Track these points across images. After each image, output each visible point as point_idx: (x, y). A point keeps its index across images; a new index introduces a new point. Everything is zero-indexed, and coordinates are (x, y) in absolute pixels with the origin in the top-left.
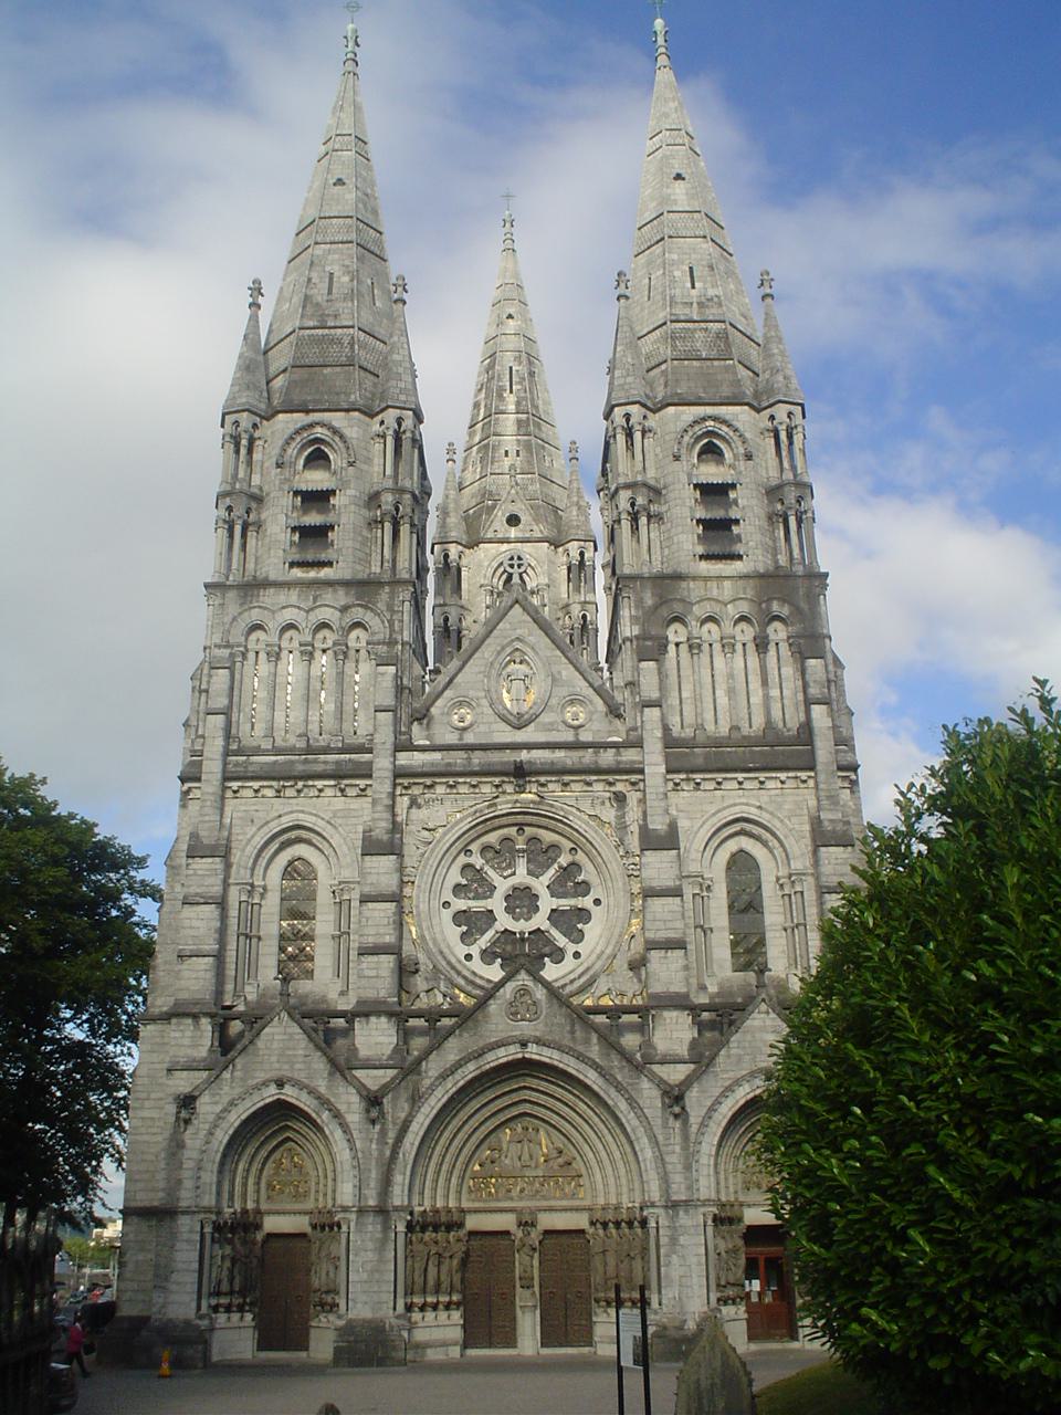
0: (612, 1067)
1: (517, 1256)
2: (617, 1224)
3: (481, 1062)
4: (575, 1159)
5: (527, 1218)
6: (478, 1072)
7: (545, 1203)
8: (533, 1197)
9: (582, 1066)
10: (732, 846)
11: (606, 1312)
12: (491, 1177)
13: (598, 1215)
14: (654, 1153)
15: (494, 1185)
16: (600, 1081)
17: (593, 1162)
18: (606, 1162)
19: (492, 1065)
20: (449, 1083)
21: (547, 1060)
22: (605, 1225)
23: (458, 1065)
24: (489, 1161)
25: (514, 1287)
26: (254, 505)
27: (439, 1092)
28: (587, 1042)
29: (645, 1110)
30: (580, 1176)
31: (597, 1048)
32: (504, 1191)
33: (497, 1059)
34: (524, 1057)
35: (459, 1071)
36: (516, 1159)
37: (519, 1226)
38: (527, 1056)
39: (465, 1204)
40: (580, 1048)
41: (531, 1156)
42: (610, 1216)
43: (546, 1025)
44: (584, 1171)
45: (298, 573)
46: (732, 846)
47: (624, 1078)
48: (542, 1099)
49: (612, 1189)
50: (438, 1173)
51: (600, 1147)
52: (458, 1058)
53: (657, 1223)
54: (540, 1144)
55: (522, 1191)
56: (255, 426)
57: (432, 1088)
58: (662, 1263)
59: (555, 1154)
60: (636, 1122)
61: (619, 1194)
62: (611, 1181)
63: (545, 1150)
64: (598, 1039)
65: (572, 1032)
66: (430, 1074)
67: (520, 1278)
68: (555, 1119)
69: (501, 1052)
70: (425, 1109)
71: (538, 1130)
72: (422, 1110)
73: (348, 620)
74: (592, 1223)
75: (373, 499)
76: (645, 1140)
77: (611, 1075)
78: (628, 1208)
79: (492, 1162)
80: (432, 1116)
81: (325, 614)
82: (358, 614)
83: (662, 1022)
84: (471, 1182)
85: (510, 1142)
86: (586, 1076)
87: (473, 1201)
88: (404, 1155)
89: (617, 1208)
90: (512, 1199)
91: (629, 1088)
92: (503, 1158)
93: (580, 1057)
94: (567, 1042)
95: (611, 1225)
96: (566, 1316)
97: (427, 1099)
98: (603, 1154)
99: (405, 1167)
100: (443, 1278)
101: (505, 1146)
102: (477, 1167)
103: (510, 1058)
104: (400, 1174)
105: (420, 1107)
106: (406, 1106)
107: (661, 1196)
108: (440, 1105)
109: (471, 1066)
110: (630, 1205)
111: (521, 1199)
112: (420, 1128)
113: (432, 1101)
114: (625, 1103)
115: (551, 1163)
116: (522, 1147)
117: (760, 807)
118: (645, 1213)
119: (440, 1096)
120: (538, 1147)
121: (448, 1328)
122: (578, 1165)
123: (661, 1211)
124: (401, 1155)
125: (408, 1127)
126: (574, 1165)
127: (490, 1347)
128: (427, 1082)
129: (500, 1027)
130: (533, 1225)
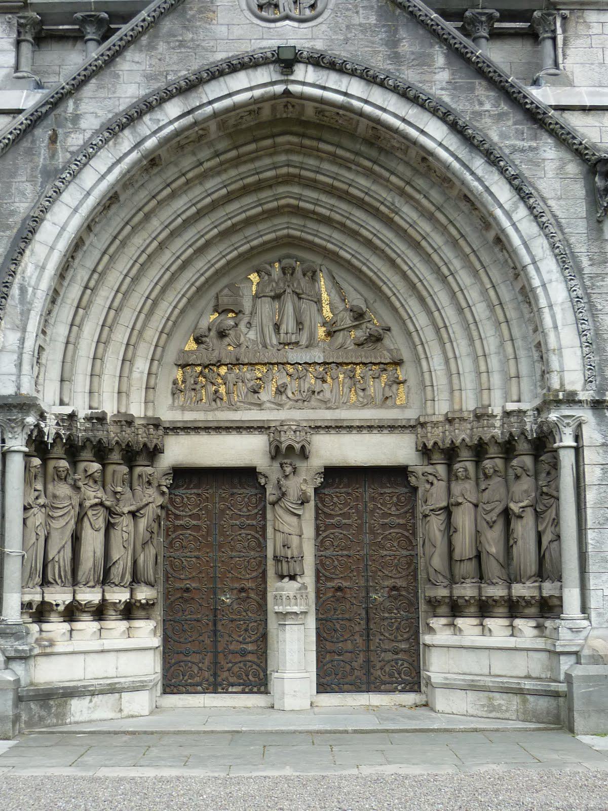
0: (478, 115)
1: (269, 516)
2: (479, 450)
3: (194, 100)
4: (389, 330)
5: (287, 439)
6: (189, 119)
7: (327, 415)
8: (303, 401)
9: (412, 113)
11: (452, 625)
12: (219, 364)
13: (434, 436)
14: (570, 290)
15: (224, 378)
16: (453, 142)
17: (428, 334)
18: (456, 330)
19: (217, 106)
20: (127, 140)
21: (340, 98)
22: (451, 454)
23: (146, 107)
24: (213, 333)
25: (264, 574)
27: (101, 162)
28: (423, 61)
29: (551, 203)
30: (398, 363)
31: (444, 76)
32: (243, 389)
33: (230, 95)
34: (287, 93)
35: (146, 118)
36: (269, 329)
37: (273, 458)
38: (295, 88)
39: (167, 415)
40: (410, 76)
41: (299, 324)
42: (462, 434)
43: (335, 28)
44: (406, 355)
47: (503, 136)
48: (326, 204)
49: (468, 381)
50: (102, 342)
51: (443, 298)
52: (143, 92)
53: (578, 438)
54: (318, 302)
55: (280, 391)
57: (87, 153)
58: (590, 524)
59: (347, 320)
60: (529, 227)
61: (482, 389)
62: (466, 364)
63: (327, 312)
64: (447, 56)
65: (392, 43)
66: (83, 124)
67: (275, 558)
68: (349, 249)
69: (240, 80)
70: (70, 196)
71: (314, 272)
72: (66, 197)
74: (425, 452)
76: (549, 266)
77: (475, 128)
78: (507, 414)
79: (222, 335)
80: (84, 210)
83: (581, 29)
84: (179, 374)
85: (257, 297)
86: (422, 132)
87: (183, 408)
88: (23, 290)
89: (481, 416)
90: (260, 406)
91: (517, 158)
92: (242, 327)
93: (406, 94)
94: (380, 63)
95: (465, 454)
96: (368, 634)
97: (74, 175)
98: (450, 314)
99: (25, 314)
100: (115, 555)
101: (247, 305)
102: (191, 345)
103: (257, 93)
104: (15, 328)
105: (58, 192)
106: (28, 188)
107: (588, 381)
108: (104, 186)
109: (174, 109)
110: (511, 407)
111: (280, 405)
112: (59, 235)
113: (88, 178)
114: (507, 187)
115: (340, 338)
116: (281, 312)
118: (553, 416)
119: (103, 170)
120: (314, 307)
121: (123, 657)
122: (395, 342)
123: (586, 414)
124: (15, 291)
125: (33, 231)
126: (387, 341)
127: (215, 692)
128: (75, 141)
129: (237, 32)
130: (304, 454)
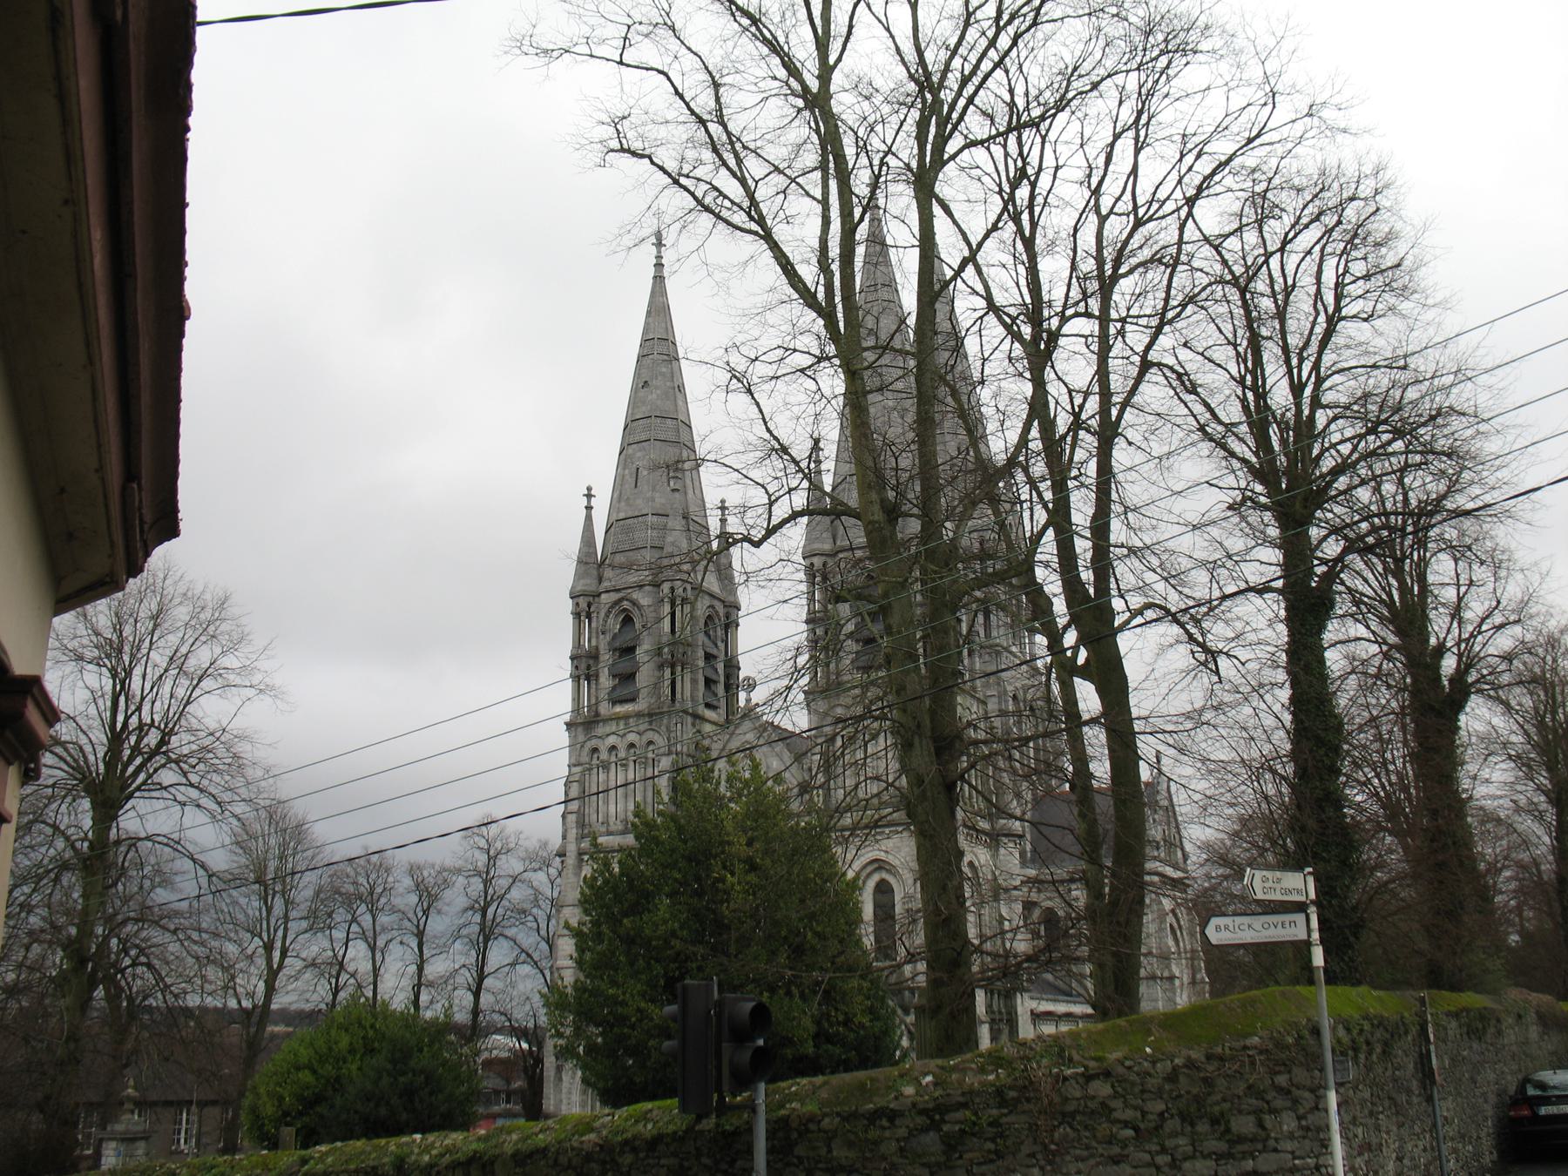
10: (876, 878)
26: (591, 662)
45: (619, 709)
46: (876, 878)
56: (589, 605)
73: (645, 739)
75: (659, 652)
81: (632, 737)
82: (650, 735)
117: (886, 852)
